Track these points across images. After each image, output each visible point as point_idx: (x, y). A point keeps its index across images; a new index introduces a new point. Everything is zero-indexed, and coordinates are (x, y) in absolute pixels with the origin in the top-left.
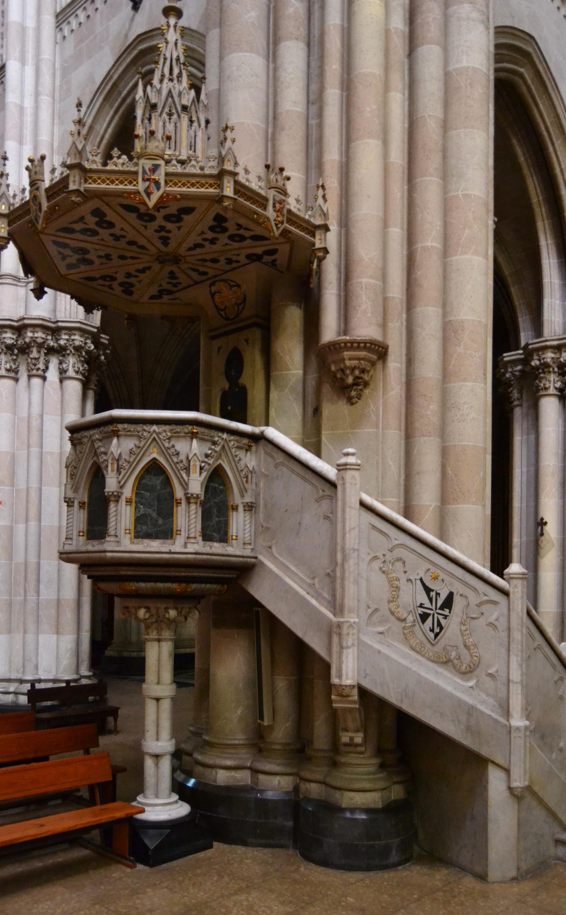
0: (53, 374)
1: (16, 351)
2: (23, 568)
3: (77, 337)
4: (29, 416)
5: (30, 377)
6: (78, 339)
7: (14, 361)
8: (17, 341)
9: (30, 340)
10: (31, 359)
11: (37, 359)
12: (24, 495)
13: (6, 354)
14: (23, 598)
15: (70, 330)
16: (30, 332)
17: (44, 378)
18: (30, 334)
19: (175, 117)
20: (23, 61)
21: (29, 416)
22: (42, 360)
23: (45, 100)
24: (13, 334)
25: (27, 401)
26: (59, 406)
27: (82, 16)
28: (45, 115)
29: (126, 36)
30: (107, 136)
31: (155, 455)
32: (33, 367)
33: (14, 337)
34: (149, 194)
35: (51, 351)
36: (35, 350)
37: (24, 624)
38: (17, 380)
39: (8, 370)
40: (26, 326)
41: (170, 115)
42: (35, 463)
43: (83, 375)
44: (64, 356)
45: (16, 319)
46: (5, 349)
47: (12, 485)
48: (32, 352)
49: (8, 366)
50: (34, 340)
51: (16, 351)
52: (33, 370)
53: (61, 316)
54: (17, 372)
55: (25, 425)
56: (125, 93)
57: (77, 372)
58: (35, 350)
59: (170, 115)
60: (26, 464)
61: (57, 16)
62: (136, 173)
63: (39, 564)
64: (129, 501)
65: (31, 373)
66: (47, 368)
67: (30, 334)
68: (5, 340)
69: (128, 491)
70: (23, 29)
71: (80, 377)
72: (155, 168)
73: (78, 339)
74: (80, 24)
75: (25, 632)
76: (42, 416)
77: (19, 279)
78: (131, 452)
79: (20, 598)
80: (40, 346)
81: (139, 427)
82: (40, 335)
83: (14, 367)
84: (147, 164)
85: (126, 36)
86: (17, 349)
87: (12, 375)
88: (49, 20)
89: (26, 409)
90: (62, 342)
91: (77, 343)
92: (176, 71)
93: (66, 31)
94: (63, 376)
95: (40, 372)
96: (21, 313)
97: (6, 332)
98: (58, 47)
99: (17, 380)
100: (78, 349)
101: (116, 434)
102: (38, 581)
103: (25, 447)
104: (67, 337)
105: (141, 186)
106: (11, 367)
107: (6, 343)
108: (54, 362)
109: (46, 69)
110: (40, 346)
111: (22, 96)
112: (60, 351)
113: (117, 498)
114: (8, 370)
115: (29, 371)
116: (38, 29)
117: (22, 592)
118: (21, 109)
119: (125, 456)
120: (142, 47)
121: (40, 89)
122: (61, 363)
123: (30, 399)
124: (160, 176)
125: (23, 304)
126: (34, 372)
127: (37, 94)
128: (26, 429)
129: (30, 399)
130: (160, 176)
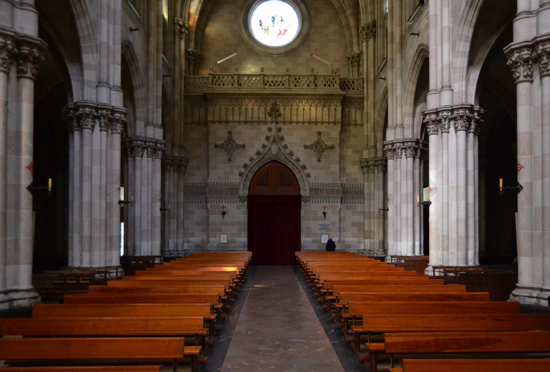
1: (531, 62)
7: (530, 69)
8: (531, 55)
9: (541, 51)
10: (543, 64)
13: (523, 66)
16: (541, 46)
24: (528, 51)
25: (540, 95)
32: (544, 70)
33: (529, 52)
39: (525, 76)
45: (530, 40)
46: (522, 62)
48: (543, 59)
49: (525, 74)
51: (531, 62)
52: (543, 72)
54: (531, 76)
55: (539, 111)
65: (543, 74)
68: (523, 56)
77: (531, 12)
83: (529, 73)
86: (532, 60)
87: (529, 79)
89: (540, 100)
97: (523, 51)
99: (532, 82)
106: (527, 73)
107: (523, 58)
114: (525, 76)
115: (541, 73)
126: (545, 73)
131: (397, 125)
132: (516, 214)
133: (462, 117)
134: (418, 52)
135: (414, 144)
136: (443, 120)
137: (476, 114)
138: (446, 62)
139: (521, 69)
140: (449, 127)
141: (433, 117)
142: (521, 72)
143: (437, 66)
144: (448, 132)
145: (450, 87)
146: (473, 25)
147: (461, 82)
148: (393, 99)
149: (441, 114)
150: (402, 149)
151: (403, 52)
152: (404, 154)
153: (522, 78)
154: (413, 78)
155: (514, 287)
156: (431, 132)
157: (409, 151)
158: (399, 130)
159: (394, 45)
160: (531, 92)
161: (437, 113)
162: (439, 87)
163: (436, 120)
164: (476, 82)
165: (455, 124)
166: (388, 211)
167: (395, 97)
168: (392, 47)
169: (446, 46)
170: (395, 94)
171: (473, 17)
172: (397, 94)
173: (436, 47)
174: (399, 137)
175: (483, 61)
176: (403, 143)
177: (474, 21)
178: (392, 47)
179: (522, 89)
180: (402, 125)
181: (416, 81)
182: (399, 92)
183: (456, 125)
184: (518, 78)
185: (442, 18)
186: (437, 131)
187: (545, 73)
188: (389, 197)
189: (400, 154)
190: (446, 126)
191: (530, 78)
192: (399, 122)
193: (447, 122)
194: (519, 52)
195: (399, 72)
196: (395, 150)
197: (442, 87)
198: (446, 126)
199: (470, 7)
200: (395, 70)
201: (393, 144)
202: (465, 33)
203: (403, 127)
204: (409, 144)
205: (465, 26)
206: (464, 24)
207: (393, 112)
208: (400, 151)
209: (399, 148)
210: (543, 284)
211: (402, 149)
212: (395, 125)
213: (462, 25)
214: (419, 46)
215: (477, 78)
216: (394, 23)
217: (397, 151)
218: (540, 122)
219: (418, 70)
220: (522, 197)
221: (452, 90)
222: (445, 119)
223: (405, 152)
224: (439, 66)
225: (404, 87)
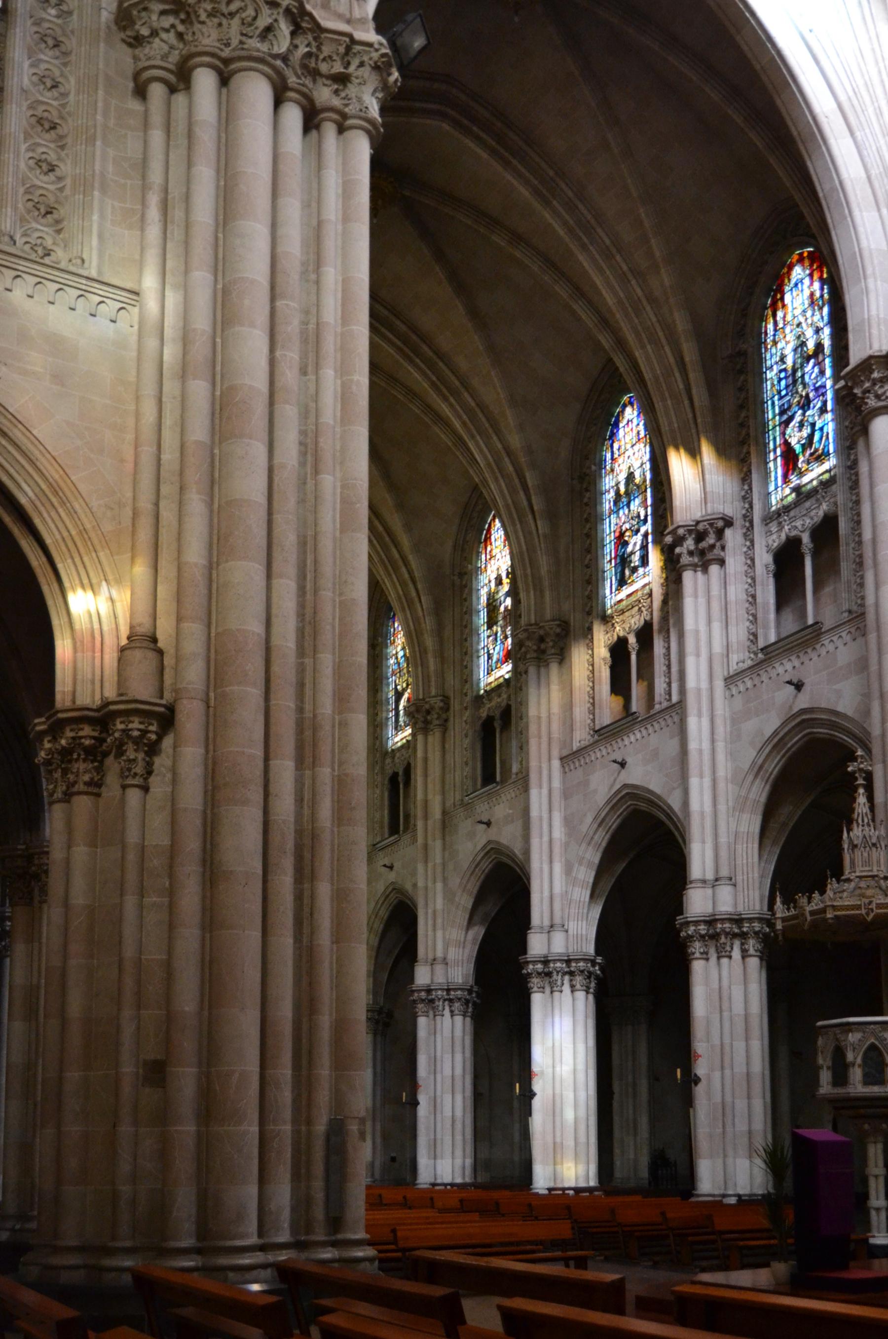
0: (736, 953)
2: (720, 1106)
3: (756, 924)
4: (720, 988)
5: (719, 958)
6: (757, 926)
7: (706, 946)
8: (708, 930)
11: (724, 944)
12: (718, 1050)
14: (721, 1130)
15: (751, 920)
17: (730, 957)
18: (719, 926)
19: (868, 849)
20: (700, 715)
21: (720, 988)
22: (729, 944)
23: (720, 746)
26: (742, 978)
27: (749, 684)
28: (721, 757)
29: (791, 707)
30: (775, 772)
31: (873, 1040)
34: (868, 914)
35: (735, 936)
36: (723, 937)
37: (724, 1150)
38: (707, 959)
39: (701, 953)
40: (716, 920)
41: (865, 847)
42: (727, 1025)
43: (761, 952)
44: (745, 939)
47: (708, 1042)
49: (702, 950)
50: (723, 930)
53: (740, 909)
54: (707, 953)
56: (789, 745)
57: (756, 951)
58: (723, 937)
59: (865, 847)
60: (719, 1025)
61: (726, 680)
62: (860, 905)
63: (733, 1102)
64: (859, 1066)
66: (732, 949)
67: (719, 926)
69: (859, 1060)
70: (699, 690)
71: (758, 954)
72: (870, 903)
73: (757, 926)
74: (747, 689)
75: (725, 1156)
76: (730, 988)
78: (860, 1040)
79: (719, 1130)
80: (727, 934)
81: (863, 1027)
82: (727, 925)
84: (867, 901)
85: (791, 707)
87: (705, 956)
88: (719, 684)
89: (717, 982)
90: (745, 930)
91: (757, 929)
92: (866, 820)
93: (734, 690)
94: (745, 954)
95: (728, 953)
96: (710, 910)
98: (727, 702)
99: (707, 959)
100: (756, 933)
101: (851, 1031)
102: (734, 1116)
103: (718, 1011)
104: (748, 925)
105: (863, 912)
108: (737, 944)
109: (719, 722)
110: (727, 934)
111: (701, 741)
112: (743, 936)
113: (853, 1064)
114: (701, 953)
115: (718, 953)
116: (711, 689)
117: (721, 1126)
118: (700, 751)
119: (856, 1042)
120: (804, 717)
121: (715, 737)
122: (742, 944)
123: (720, 975)
124: (873, 906)
125: (711, 902)
126: (723, 954)
127: (713, 741)
128: (717, 998)
129: (720, 975)
130: (873, 906)
131: (434, 960)
132: (691, 1110)
133: (582, 972)
134: (486, 850)
135: (466, 993)
136: (555, 973)
137: (597, 968)
138: (558, 888)
139: (697, 944)
140: (563, 984)
141: (539, 967)
142: (697, 947)
143: (542, 893)
144: (561, 992)
145: (563, 926)
146: (601, 849)
147: (580, 923)
148: (426, 913)
149: (552, 965)
150: (445, 1000)
151: (447, 838)
152: (447, 1008)
153: (697, 955)
154: (469, 886)
155: (693, 1195)
156: (535, 989)
157: (457, 1005)
158: (439, 969)
159: (430, 822)
160: (706, 970)
161: (546, 962)
162: (547, 923)
163: (543, 972)
164: (597, 921)
165: (571, 980)
166: (419, 1107)
167: (430, 911)
168: (426, 825)
169: (558, 868)
170: (431, 905)
171: (602, 838)
172: (435, 906)
173: (541, 864)
174: (440, 979)
175: (606, 894)
176: (448, 990)
177: (604, 844)
178: (426, 825)
179: (698, 966)
180: (445, 959)
181: (475, 891)
182: (439, 903)
183: (574, 983)
184: (693, 954)
185: (550, 826)
186: (543, 988)
187: (723, 954)
188: (420, 1082)
189: (441, 1008)
190: (559, 983)
191: (706, 957)
192: (440, 954)
193: (560, 977)
194: (696, 926)
195: (439, 869)
196: (432, 1001)
197: (552, 926)
198: (559, 983)
199: (600, 825)
200: (430, 865)
201: (429, 991)
202: (588, 856)
203: (447, 964)
204: (459, 992)
205: (590, 848)
206: (589, 844)
207: (427, 936)
208: (441, 1003)
209: (439, 999)
210: (726, 1189)
211: (445, 1000)
212: (431, 956)
213: (584, 845)
214: (489, 842)
215: (598, 916)
216: (430, 786)
217: (437, 1003)
218: (718, 1008)
219: (482, 877)
220: (700, 1091)
221: (567, 931)
222: (558, 972)
223: (450, 1007)
224: (546, 893)
225: (449, 896)
